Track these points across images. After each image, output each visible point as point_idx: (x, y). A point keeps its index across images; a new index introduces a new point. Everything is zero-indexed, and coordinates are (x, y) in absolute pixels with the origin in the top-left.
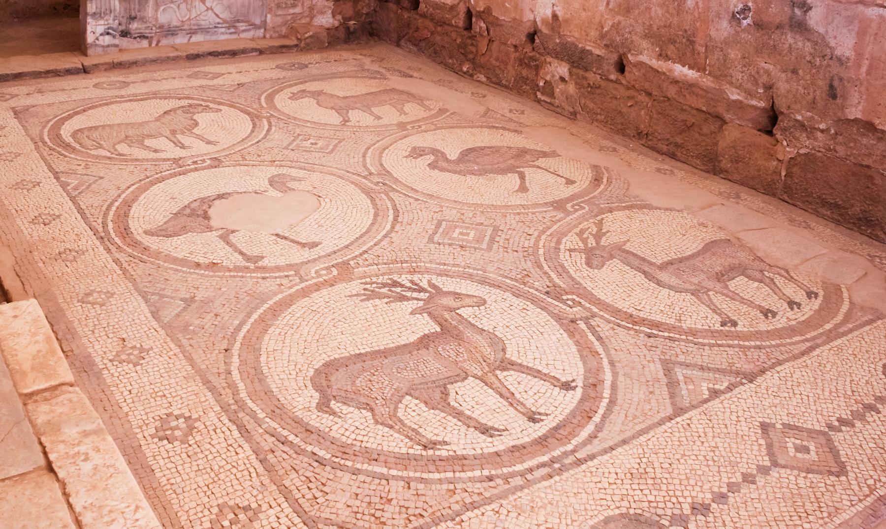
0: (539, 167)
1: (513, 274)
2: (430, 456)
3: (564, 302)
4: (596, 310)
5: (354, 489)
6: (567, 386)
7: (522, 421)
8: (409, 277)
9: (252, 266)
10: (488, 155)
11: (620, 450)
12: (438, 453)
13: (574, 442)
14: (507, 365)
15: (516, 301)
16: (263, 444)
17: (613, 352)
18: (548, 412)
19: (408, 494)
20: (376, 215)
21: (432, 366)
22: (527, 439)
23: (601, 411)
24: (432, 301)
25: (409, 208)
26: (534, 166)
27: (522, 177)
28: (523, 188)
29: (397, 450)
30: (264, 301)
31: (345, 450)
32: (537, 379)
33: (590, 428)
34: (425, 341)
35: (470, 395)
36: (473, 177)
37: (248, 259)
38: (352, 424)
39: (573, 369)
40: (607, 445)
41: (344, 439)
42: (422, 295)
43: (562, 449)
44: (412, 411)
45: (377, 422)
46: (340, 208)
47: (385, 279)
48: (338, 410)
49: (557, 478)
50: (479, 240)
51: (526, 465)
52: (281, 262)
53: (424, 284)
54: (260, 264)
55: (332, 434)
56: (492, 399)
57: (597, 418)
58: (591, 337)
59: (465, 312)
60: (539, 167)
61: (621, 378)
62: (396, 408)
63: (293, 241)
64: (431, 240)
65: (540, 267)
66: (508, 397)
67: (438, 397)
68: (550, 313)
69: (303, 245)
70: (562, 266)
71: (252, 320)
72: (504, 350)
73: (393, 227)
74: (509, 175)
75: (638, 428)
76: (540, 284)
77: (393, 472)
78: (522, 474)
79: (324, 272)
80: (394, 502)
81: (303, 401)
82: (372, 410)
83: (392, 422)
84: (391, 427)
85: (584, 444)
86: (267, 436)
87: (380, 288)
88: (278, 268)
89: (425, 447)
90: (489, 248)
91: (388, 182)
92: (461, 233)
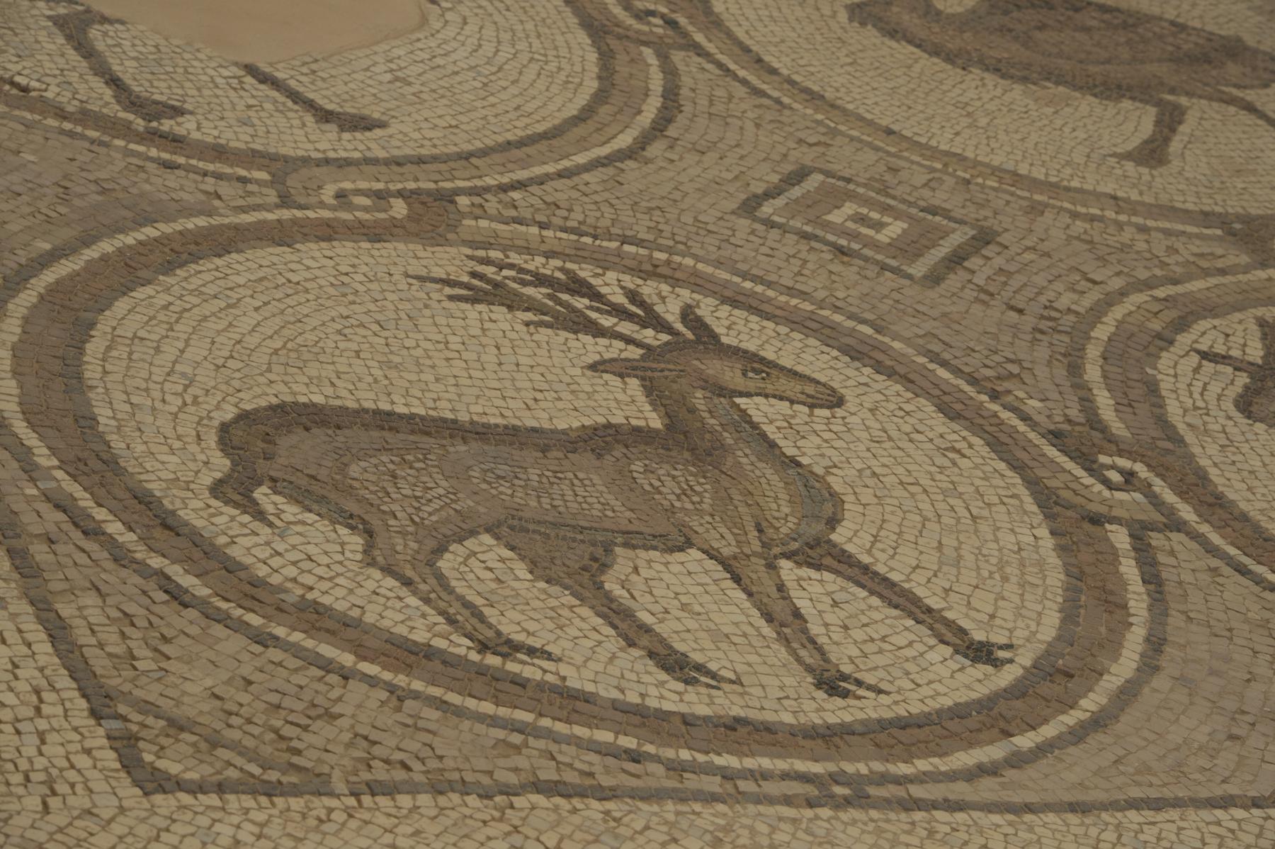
0: (1250, 108)
1: (972, 363)
2: (492, 668)
3: (1092, 469)
4: (1187, 513)
5: (246, 670)
6: (982, 653)
7: (797, 681)
8: (629, 281)
9: (140, 124)
10: (1088, 30)
11: (1051, 817)
12: (512, 667)
13: (923, 765)
14: (819, 553)
15: (939, 423)
16: (28, 518)
17: (1175, 620)
18: (883, 686)
19: (388, 718)
20: (601, 97)
21: (591, 493)
22: (788, 718)
23: (1048, 731)
24: (676, 356)
25: (719, 108)
26: (1231, 101)
27: (1170, 120)
28: (1152, 153)
29: (401, 630)
30: (151, 221)
31: (254, 591)
32: (896, 612)
33: (994, 752)
34: (601, 439)
35: (679, 591)
36: (990, 79)
37: (134, 103)
38: (300, 549)
39: (1029, 621)
40: (1017, 798)
41: (262, 571)
42: (648, 335)
43: (878, 766)
44: (482, 566)
45: (373, 563)
46: (488, 49)
47: (551, 267)
48: (270, 509)
49: (825, 812)
50: (908, 248)
51: (749, 763)
52: (237, 138)
53: (671, 311)
54: (167, 125)
55: (235, 552)
56: (735, 611)
57: (1025, 741)
58: (1129, 568)
59: (757, 408)
60: (1250, 108)
61: (1160, 682)
62: (441, 550)
63: (295, 96)
64: (750, 207)
65: (1075, 369)
66: (787, 622)
67: (578, 561)
68: (1033, 484)
69: (325, 116)
70: (1153, 388)
71: (91, 253)
72: (833, 523)
73: (643, 142)
74: (1126, 104)
75: (1136, 793)
76: (1043, 399)
77: (370, 669)
78: (728, 775)
79: (365, 201)
80: (344, 722)
81: (178, 462)
82: (370, 533)
83: (420, 574)
84: (408, 583)
85: (952, 776)
86: (45, 508)
87: (524, 283)
88: (219, 152)
89: (483, 647)
90: (934, 278)
91: (682, 21)
92: (862, 220)
